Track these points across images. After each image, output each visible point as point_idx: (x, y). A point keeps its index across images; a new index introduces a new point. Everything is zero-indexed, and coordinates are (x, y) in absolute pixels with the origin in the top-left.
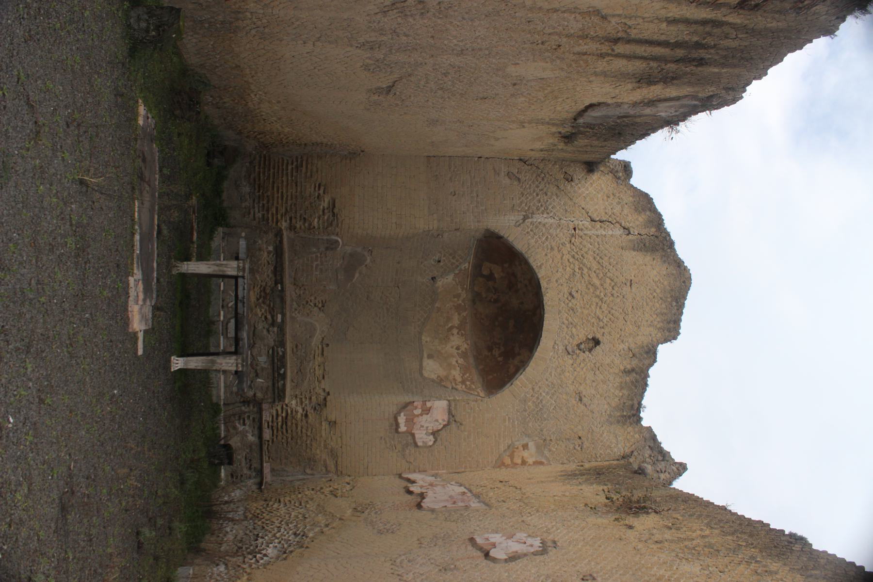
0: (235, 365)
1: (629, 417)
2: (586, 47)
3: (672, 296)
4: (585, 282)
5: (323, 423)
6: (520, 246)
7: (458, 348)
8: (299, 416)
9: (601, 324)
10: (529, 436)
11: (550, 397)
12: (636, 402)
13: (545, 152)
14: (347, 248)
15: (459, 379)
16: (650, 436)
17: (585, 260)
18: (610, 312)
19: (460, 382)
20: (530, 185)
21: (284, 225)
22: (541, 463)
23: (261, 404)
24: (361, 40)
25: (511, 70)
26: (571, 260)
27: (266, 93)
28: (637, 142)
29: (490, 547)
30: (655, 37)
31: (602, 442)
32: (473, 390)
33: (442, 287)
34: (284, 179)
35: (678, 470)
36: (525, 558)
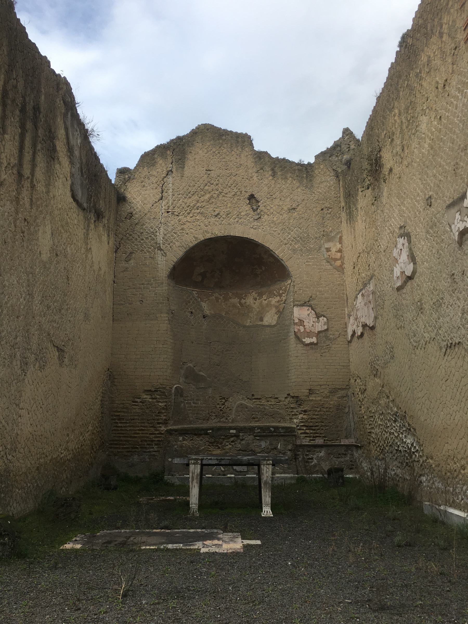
0: (268, 466)
1: (308, 172)
2: (25, 199)
3: (218, 139)
4: (207, 205)
6: (180, 253)
7: (255, 299)
9: (239, 193)
10: (320, 248)
11: (292, 231)
12: (296, 168)
13: (110, 233)
14: (181, 381)
16: (322, 156)
17: (191, 205)
18: (230, 187)
19: (280, 298)
20: (135, 245)
21: (163, 428)
22: (341, 238)
23: (297, 446)
24: (19, 372)
25: (45, 257)
26: (191, 215)
27: (60, 445)
28: (101, 162)
29: (404, 275)
30: (17, 144)
31: (325, 193)
32: (286, 288)
34: (128, 429)
35: (348, 135)
36: (413, 249)
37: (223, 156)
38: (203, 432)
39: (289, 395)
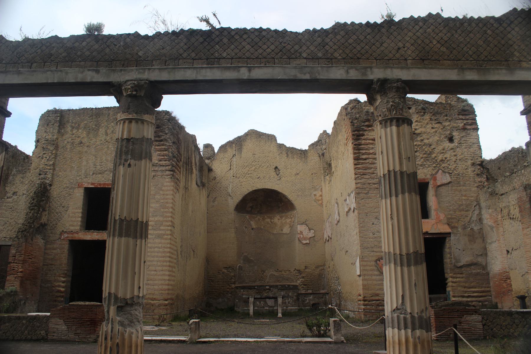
1: (305, 154)
3: (259, 138)
5: (306, 271)
6: (240, 198)
7: (279, 220)
8: (303, 280)
12: (299, 152)
15: (290, 220)
16: (312, 146)
21: (233, 286)
22: (321, 189)
26: (245, 178)
31: (314, 165)
32: (294, 214)
33: (255, 225)
34: (216, 286)
37: (262, 146)
38: (253, 288)
39: (295, 269)
